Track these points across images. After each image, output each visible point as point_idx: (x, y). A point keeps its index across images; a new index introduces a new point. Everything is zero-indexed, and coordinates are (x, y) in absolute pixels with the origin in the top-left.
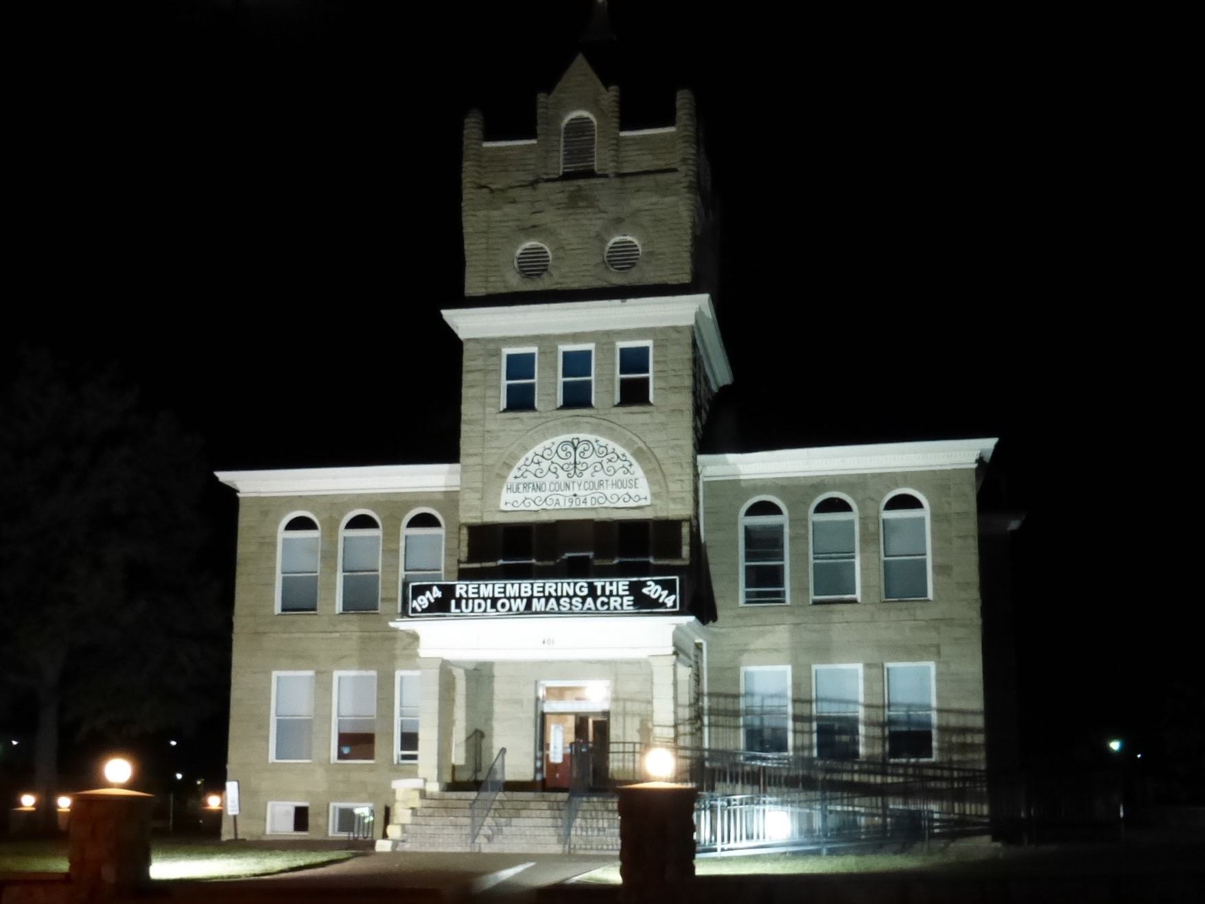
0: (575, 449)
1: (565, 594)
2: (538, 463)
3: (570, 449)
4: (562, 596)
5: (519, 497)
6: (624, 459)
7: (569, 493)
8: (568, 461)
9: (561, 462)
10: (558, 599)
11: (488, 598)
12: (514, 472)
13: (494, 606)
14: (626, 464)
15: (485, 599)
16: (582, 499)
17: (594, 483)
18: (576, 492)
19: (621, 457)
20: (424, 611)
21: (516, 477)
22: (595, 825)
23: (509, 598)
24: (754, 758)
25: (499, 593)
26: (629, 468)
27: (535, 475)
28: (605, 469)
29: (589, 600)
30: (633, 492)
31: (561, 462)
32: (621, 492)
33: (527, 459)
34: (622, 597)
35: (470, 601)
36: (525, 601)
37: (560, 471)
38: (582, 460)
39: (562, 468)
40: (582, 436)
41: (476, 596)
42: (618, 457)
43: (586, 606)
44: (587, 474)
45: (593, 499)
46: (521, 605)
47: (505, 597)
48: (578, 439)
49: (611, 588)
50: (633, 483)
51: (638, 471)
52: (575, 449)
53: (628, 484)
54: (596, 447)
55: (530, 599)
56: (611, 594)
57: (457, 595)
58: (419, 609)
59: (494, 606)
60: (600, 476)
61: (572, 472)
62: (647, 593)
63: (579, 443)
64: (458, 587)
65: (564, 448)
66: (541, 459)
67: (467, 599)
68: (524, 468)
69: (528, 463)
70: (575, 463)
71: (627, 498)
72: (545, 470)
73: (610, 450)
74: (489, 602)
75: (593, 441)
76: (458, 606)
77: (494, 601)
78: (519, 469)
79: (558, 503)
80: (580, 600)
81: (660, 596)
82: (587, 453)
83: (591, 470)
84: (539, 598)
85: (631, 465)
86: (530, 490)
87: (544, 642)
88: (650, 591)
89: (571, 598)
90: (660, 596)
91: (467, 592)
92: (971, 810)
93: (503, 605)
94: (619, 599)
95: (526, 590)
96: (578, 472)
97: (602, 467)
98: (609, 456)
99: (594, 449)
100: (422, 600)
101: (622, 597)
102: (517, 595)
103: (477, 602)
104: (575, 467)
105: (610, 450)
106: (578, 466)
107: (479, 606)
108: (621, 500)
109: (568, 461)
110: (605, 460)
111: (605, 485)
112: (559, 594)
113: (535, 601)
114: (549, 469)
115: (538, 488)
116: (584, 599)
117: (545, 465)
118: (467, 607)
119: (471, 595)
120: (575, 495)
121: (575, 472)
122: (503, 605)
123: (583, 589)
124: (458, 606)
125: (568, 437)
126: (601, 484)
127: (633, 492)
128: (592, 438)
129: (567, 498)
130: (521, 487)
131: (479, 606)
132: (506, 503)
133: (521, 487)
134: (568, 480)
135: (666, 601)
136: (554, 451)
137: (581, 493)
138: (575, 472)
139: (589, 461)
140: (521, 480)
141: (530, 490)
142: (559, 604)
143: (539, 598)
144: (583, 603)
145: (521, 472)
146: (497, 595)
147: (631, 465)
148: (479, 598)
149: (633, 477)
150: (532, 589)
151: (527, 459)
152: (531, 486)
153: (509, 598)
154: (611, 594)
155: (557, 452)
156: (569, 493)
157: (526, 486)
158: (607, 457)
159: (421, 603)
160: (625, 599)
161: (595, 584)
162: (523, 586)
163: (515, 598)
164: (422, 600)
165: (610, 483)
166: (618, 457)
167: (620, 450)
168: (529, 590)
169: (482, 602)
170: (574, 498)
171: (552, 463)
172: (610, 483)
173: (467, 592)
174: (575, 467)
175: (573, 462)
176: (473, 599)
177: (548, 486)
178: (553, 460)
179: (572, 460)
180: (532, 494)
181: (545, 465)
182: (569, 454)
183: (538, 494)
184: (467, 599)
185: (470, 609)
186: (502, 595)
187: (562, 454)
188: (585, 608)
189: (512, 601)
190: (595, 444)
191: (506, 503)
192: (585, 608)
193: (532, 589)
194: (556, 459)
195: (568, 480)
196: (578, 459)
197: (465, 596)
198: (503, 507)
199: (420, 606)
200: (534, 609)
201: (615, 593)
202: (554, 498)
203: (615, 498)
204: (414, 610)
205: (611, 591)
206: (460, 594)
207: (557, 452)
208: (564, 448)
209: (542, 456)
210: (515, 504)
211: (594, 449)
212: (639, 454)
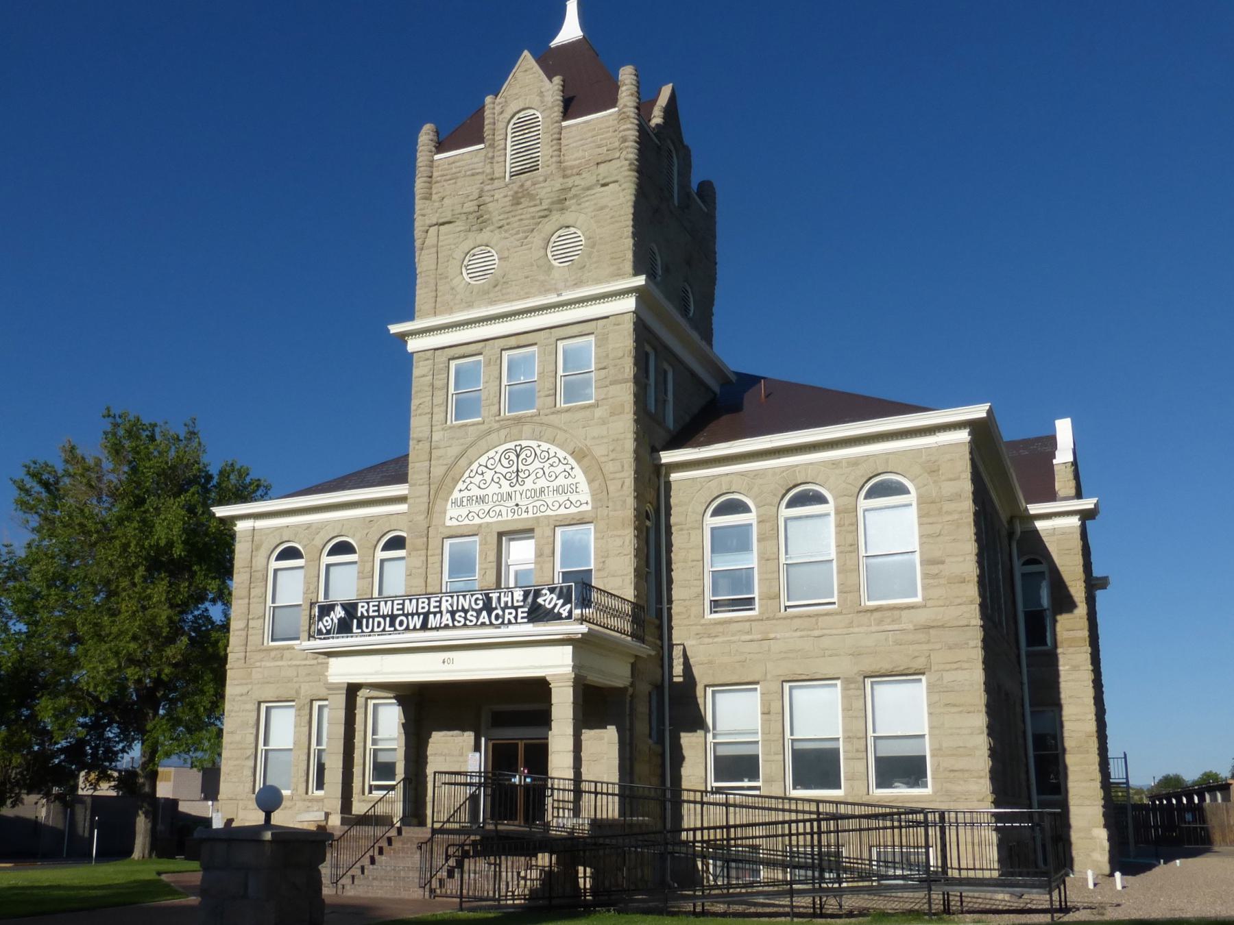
0: (518, 456)
1: (460, 608)
2: (482, 474)
3: (513, 457)
4: (458, 611)
5: (463, 511)
6: (565, 462)
7: (511, 504)
8: (510, 470)
9: (504, 471)
10: (466, 612)
11: (388, 615)
12: (460, 485)
13: (392, 624)
14: (568, 468)
15: (384, 617)
16: (524, 508)
17: (535, 491)
18: (518, 500)
19: (562, 460)
20: (328, 632)
21: (461, 491)
22: (534, 863)
23: (407, 616)
24: (500, 775)
25: (398, 610)
26: (570, 471)
27: (479, 487)
28: (547, 474)
29: (484, 613)
30: (574, 498)
31: (504, 471)
32: (562, 498)
33: (472, 471)
34: (516, 608)
35: (371, 620)
36: (422, 617)
37: (503, 481)
38: (524, 468)
39: (505, 477)
40: (524, 443)
41: (376, 614)
42: (560, 461)
43: (481, 620)
44: (529, 482)
45: (535, 508)
46: (417, 622)
47: (403, 615)
48: (520, 445)
49: (506, 599)
50: (574, 488)
51: (579, 476)
52: (518, 456)
53: (569, 489)
54: (538, 452)
55: (426, 615)
56: (506, 607)
57: (359, 615)
58: (324, 631)
59: (392, 624)
60: (542, 482)
61: (514, 481)
62: (543, 603)
63: (521, 449)
64: (360, 605)
65: (507, 457)
66: (485, 469)
67: (368, 618)
68: (468, 481)
69: (472, 475)
70: (518, 471)
71: (568, 504)
72: (489, 481)
73: (552, 454)
74: (388, 619)
75: (535, 447)
76: (359, 626)
77: (393, 618)
78: (464, 481)
79: (500, 514)
80: (475, 614)
81: (556, 605)
82: (530, 460)
83: (533, 476)
84: (435, 614)
85: (572, 468)
86: (474, 502)
87: (444, 662)
88: (545, 601)
89: (466, 612)
90: (556, 605)
91: (368, 611)
92: (709, 836)
93: (401, 623)
94: (513, 611)
95: (423, 605)
96: (520, 479)
97: (544, 473)
98: (551, 461)
99: (536, 454)
100: (327, 621)
101: (516, 608)
102: (415, 611)
103: (377, 620)
104: (518, 475)
105: (552, 454)
106: (521, 474)
107: (379, 624)
108: (563, 506)
109: (510, 470)
110: (547, 465)
111: (546, 492)
112: (455, 608)
113: (431, 616)
114: (493, 480)
115: (481, 500)
116: (479, 612)
117: (489, 475)
118: (367, 627)
119: (371, 614)
120: (517, 505)
121: (517, 480)
122: (401, 623)
123: (478, 602)
124: (359, 626)
125: (511, 445)
126: (542, 491)
127: (574, 498)
128: (534, 444)
129: (509, 509)
130: (465, 500)
131: (379, 624)
132: (451, 518)
133: (465, 500)
134: (510, 490)
135: (561, 611)
136: (497, 460)
137: (524, 503)
138: (517, 480)
139: (531, 468)
140: (466, 493)
141: (474, 502)
142: (453, 619)
143: (435, 614)
144: (478, 618)
145: (466, 485)
146: (396, 612)
147: (572, 468)
148: (379, 616)
149: (574, 481)
150: (429, 604)
151: (472, 471)
152: (474, 498)
153: (407, 616)
154: (506, 607)
155: (500, 460)
156: (511, 504)
157: (470, 499)
158: (549, 461)
159: (326, 624)
160: (520, 610)
161: (490, 595)
162: (420, 601)
163: (413, 615)
164: (327, 621)
165: (551, 489)
166: (560, 461)
167: (561, 454)
168: (425, 605)
169: (381, 620)
170: (516, 508)
171: (496, 472)
172: (551, 489)
173: (368, 611)
174: (518, 475)
175: (515, 470)
176: (373, 617)
177: (490, 499)
178: (497, 470)
179: (514, 468)
180: (475, 508)
181: (489, 475)
182: (511, 462)
183: (482, 506)
184: (368, 618)
185: (370, 629)
186: (401, 612)
187: (505, 462)
188: (479, 623)
189: (410, 617)
190: (537, 449)
191: (451, 518)
192: (479, 623)
193: (429, 604)
194: (499, 469)
195: (510, 490)
196: (521, 467)
197: (366, 614)
198: (448, 523)
199: (325, 627)
200: (429, 626)
201: (510, 604)
202: (497, 509)
203: (557, 505)
204: (320, 632)
205: (506, 603)
206: (362, 613)
207: (500, 460)
208: (507, 457)
209: (486, 467)
210: (460, 519)
211: (536, 454)
212: (580, 455)
